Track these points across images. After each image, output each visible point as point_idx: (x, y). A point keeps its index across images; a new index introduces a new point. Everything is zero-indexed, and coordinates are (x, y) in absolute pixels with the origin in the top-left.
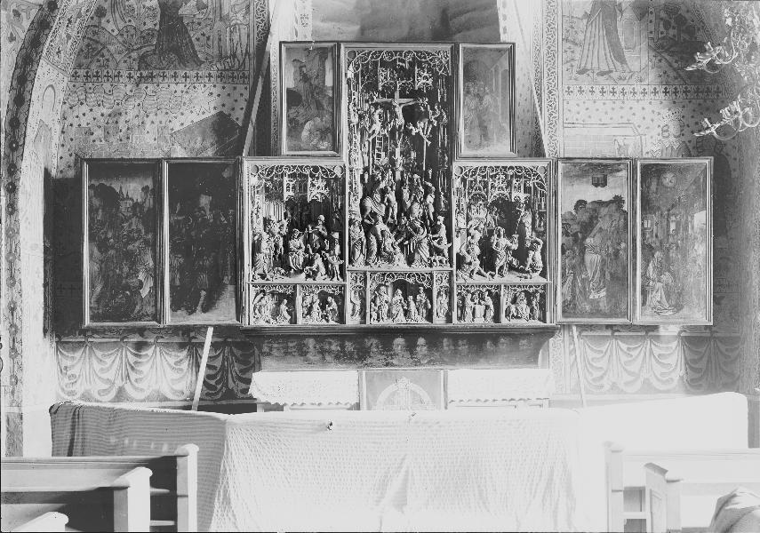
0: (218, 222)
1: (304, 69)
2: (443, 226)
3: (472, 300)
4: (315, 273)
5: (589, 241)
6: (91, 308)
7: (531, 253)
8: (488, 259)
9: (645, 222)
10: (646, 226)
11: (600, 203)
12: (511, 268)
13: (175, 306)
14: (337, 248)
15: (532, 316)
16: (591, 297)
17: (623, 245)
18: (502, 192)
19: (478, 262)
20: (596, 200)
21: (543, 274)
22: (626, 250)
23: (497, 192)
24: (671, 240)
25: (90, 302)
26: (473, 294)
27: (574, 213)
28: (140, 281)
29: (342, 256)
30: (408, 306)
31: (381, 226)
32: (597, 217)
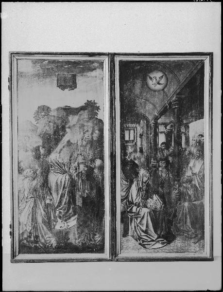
5: (53, 157)
9: (127, 133)
10: (127, 138)
16: (58, 227)
17: (98, 162)
20: (63, 105)
22: (102, 168)
24: (159, 155)
32: (63, 128)
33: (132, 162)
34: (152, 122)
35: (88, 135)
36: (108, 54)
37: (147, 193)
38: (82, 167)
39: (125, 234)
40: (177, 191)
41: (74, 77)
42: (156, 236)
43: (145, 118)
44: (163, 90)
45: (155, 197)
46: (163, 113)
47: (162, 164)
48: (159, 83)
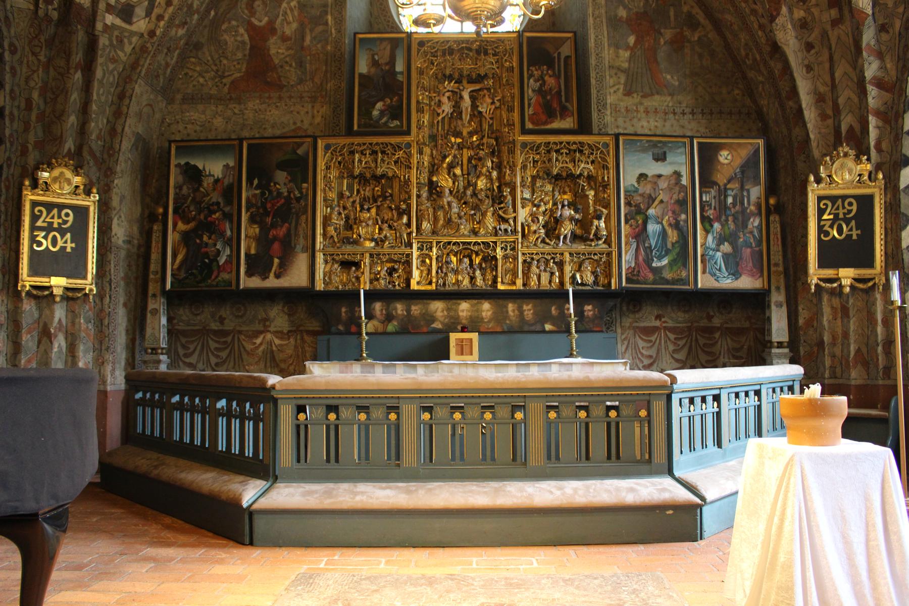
0: (292, 195)
1: (376, 57)
2: (509, 197)
3: (538, 267)
4: (383, 241)
5: (651, 212)
6: (172, 275)
7: (596, 222)
8: (552, 229)
10: (704, 199)
11: (660, 176)
12: (575, 237)
13: (249, 274)
14: (405, 220)
15: (596, 283)
16: (654, 265)
17: (683, 216)
18: (566, 165)
19: (543, 231)
21: (608, 242)
22: (686, 221)
23: (561, 165)
24: (728, 212)
25: (172, 270)
26: (538, 261)
27: (636, 185)
28: (218, 250)
29: (409, 225)
30: (474, 273)
31: (447, 198)
33: (708, 217)
34: (722, 187)
35: (675, 197)
36: (689, 137)
37: (721, 240)
38: (671, 219)
39: (704, 272)
40: (741, 240)
41: (665, 153)
42: (727, 274)
43: (716, 183)
44: (730, 164)
45: (726, 244)
46: (729, 181)
47: (730, 218)
48: (726, 159)
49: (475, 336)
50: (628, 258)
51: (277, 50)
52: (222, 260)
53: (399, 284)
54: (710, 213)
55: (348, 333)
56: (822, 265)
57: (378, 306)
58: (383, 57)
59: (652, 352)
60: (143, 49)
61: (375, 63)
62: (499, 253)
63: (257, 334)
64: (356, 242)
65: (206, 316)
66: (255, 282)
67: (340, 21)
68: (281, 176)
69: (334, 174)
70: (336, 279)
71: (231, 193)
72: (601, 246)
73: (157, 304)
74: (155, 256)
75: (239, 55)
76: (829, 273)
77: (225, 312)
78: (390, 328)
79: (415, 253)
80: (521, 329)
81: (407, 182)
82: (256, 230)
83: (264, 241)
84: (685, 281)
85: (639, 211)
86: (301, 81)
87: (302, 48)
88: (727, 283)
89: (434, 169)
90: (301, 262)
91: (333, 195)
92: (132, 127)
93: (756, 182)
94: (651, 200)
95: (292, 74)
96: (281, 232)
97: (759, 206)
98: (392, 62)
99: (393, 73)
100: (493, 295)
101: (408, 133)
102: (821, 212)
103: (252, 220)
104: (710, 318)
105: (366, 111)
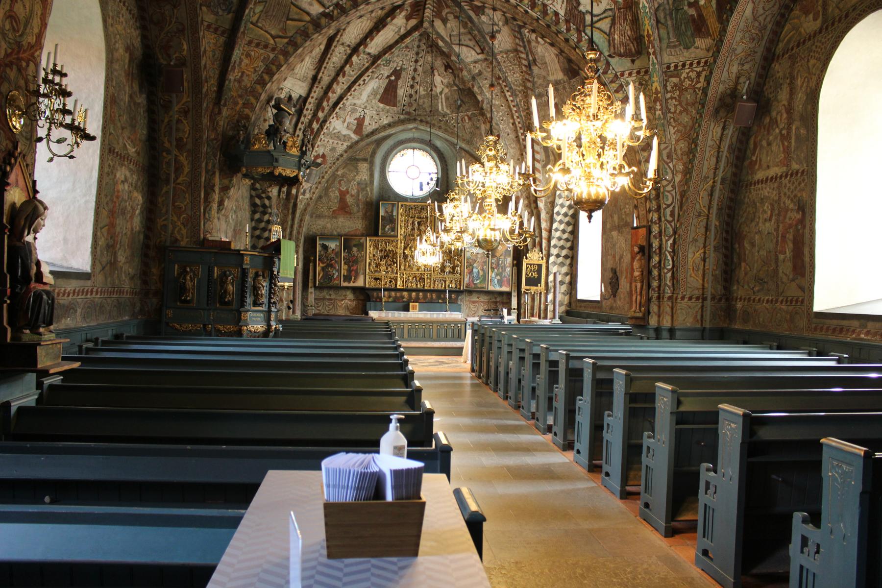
5: (475, 265)
21: (460, 274)
37: (497, 275)
49: (417, 304)
50: (466, 280)
51: (349, 199)
52: (335, 277)
53: (393, 287)
54: (494, 266)
55: (376, 301)
56: (526, 285)
57: (386, 293)
58: (389, 210)
59: (475, 309)
60: (308, 204)
61: (386, 212)
62: (426, 277)
63: (342, 300)
64: (379, 272)
65: (325, 294)
66: (346, 284)
67: (372, 190)
68: (355, 249)
69: (372, 248)
70: (372, 284)
71: (338, 254)
72: (458, 275)
73: (311, 290)
74: (311, 274)
75: (336, 201)
76: (528, 287)
77: (331, 292)
78: (390, 300)
79: (399, 276)
80: (431, 301)
81: (396, 253)
82: (346, 267)
83: (349, 271)
84: (483, 288)
85: (471, 265)
86: (358, 212)
87: (359, 200)
88: (498, 289)
89: (405, 248)
90: (361, 278)
91: (371, 256)
92: (304, 230)
93: (510, 256)
94: (475, 261)
95: (355, 209)
96: (355, 268)
97: (509, 264)
98: (392, 212)
99: (392, 216)
100: (423, 291)
101: (397, 237)
102: (527, 268)
103: (345, 263)
104: (496, 298)
105: (383, 229)
